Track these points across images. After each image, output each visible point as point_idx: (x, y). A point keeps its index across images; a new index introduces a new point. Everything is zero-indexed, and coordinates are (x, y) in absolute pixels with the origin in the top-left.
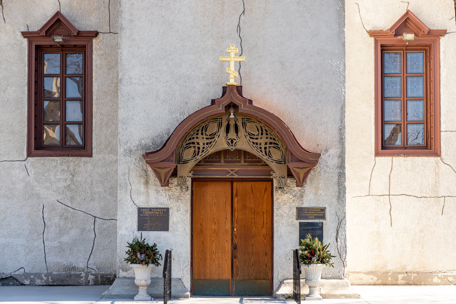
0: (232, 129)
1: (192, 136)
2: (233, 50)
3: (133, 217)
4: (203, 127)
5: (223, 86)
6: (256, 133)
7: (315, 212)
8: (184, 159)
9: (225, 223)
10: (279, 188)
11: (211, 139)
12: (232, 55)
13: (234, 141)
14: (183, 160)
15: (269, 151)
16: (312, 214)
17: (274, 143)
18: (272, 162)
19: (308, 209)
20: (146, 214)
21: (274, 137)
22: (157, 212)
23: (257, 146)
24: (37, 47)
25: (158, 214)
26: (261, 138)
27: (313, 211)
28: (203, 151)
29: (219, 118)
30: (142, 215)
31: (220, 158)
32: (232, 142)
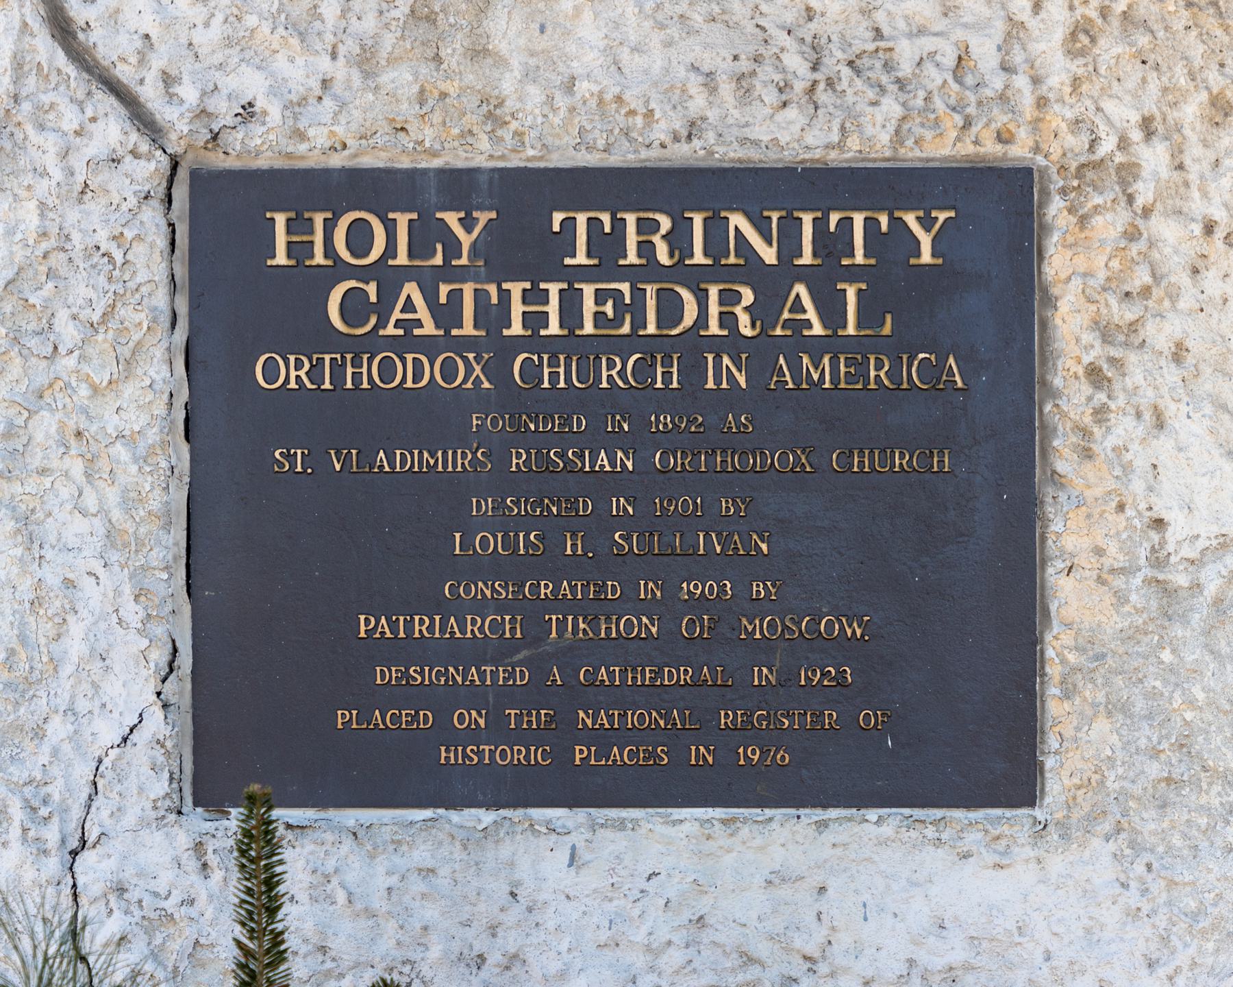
3: (45, 426)
20: (408, 341)
22: (697, 280)
25: (732, 343)
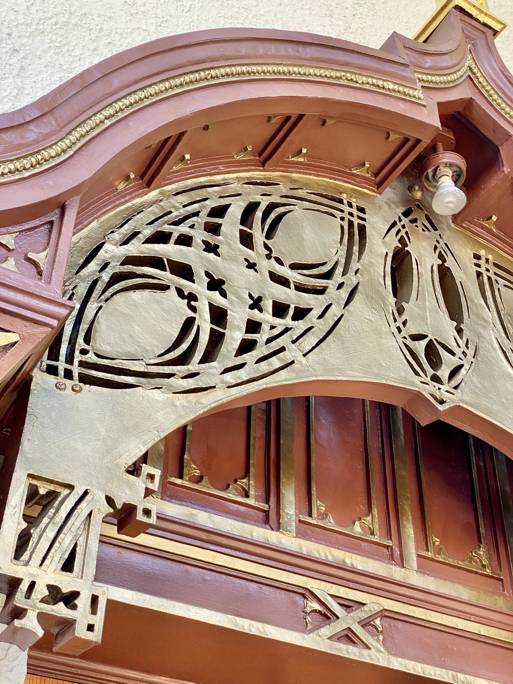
1: (177, 223)
14: (91, 358)
29: (350, 205)
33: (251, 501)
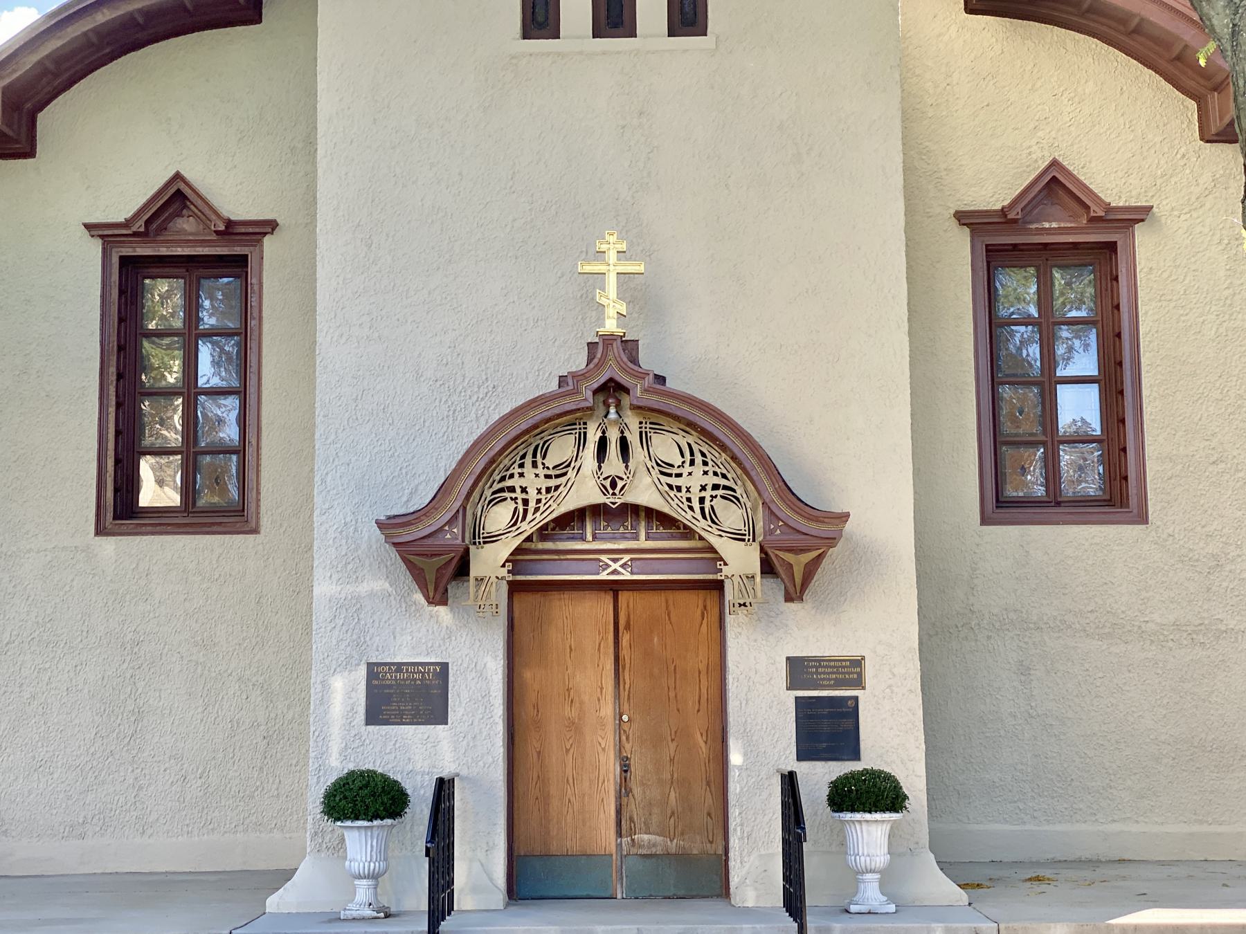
0: (613, 449)
1: (507, 470)
2: (612, 244)
4: (537, 447)
5: (589, 341)
6: (677, 460)
7: (835, 670)
8: (487, 530)
9: (599, 700)
10: (740, 605)
11: (557, 476)
12: (612, 256)
13: (620, 484)
14: (486, 535)
15: (712, 506)
16: (829, 673)
17: (725, 488)
18: (721, 536)
19: (819, 661)
21: (724, 471)
22: (416, 673)
23: (679, 495)
24: (124, 260)
25: (419, 679)
26: (690, 474)
27: (831, 667)
28: (537, 510)
29: (580, 424)
30: (376, 682)
31: (583, 527)
32: (614, 485)
33: (576, 532)
